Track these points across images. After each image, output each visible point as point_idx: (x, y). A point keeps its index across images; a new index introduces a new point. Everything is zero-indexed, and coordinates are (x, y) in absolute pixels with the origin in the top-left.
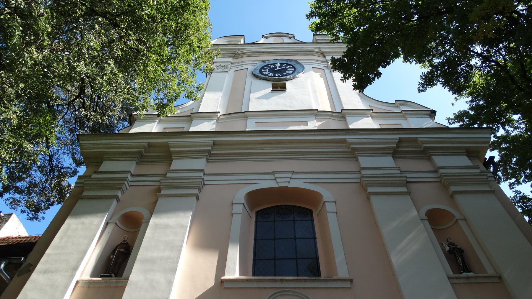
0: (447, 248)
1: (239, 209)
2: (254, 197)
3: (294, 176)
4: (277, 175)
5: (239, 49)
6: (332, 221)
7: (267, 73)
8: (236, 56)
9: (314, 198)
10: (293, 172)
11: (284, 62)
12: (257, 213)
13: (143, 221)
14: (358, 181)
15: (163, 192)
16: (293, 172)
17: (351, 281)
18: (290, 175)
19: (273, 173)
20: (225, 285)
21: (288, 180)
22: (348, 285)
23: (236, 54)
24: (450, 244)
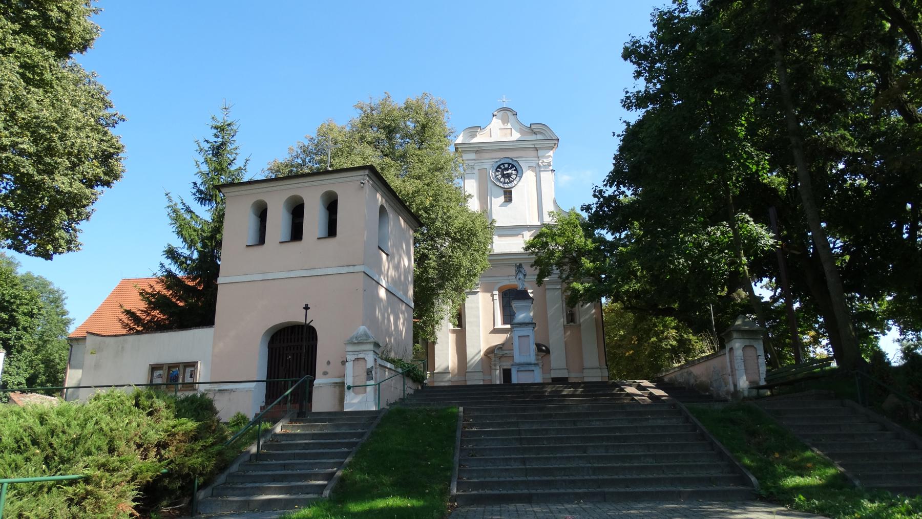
8: (477, 152)
11: (510, 162)
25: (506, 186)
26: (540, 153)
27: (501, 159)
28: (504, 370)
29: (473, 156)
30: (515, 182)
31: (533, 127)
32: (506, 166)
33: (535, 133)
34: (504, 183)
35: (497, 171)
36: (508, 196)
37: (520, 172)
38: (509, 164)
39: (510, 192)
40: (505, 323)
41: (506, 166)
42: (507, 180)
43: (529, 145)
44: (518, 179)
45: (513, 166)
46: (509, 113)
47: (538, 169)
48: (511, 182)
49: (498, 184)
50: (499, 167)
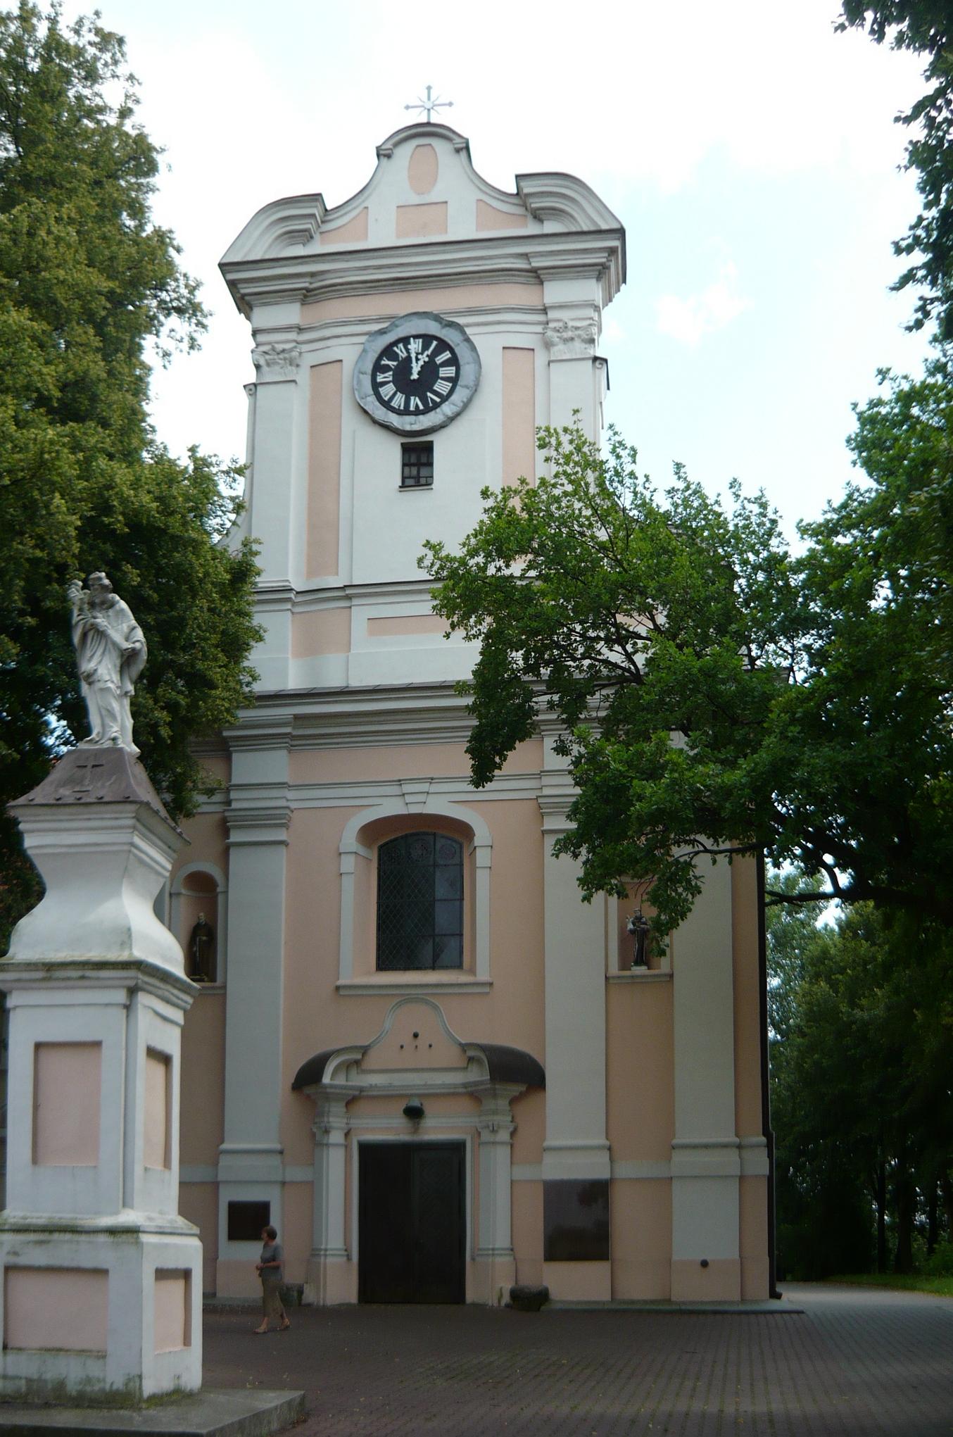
0: (630, 926)
1: (348, 864)
2: (370, 832)
3: (434, 788)
4: (407, 788)
5: (313, 275)
6: (482, 879)
7: (388, 391)
8: (307, 296)
9: (463, 831)
10: (431, 780)
11: (433, 328)
12: (381, 848)
13: (219, 889)
14: (533, 795)
15: (235, 837)
16: (431, 780)
17: (491, 984)
18: (425, 787)
19: (400, 782)
20: (342, 992)
21: (421, 798)
22: (487, 990)
25: (408, 423)
26: (555, 292)
27: (394, 320)
28: (367, 1151)
29: (290, 314)
30: (447, 409)
32: (415, 346)
34: (406, 412)
35: (378, 368)
36: (417, 461)
37: (467, 370)
38: (427, 339)
39: (428, 448)
40: (384, 963)
42: (415, 401)
44: (459, 396)
45: (443, 346)
46: (438, 144)
47: (541, 358)
48: (427, 410)
49: (380, 413)
50: (388, 352)
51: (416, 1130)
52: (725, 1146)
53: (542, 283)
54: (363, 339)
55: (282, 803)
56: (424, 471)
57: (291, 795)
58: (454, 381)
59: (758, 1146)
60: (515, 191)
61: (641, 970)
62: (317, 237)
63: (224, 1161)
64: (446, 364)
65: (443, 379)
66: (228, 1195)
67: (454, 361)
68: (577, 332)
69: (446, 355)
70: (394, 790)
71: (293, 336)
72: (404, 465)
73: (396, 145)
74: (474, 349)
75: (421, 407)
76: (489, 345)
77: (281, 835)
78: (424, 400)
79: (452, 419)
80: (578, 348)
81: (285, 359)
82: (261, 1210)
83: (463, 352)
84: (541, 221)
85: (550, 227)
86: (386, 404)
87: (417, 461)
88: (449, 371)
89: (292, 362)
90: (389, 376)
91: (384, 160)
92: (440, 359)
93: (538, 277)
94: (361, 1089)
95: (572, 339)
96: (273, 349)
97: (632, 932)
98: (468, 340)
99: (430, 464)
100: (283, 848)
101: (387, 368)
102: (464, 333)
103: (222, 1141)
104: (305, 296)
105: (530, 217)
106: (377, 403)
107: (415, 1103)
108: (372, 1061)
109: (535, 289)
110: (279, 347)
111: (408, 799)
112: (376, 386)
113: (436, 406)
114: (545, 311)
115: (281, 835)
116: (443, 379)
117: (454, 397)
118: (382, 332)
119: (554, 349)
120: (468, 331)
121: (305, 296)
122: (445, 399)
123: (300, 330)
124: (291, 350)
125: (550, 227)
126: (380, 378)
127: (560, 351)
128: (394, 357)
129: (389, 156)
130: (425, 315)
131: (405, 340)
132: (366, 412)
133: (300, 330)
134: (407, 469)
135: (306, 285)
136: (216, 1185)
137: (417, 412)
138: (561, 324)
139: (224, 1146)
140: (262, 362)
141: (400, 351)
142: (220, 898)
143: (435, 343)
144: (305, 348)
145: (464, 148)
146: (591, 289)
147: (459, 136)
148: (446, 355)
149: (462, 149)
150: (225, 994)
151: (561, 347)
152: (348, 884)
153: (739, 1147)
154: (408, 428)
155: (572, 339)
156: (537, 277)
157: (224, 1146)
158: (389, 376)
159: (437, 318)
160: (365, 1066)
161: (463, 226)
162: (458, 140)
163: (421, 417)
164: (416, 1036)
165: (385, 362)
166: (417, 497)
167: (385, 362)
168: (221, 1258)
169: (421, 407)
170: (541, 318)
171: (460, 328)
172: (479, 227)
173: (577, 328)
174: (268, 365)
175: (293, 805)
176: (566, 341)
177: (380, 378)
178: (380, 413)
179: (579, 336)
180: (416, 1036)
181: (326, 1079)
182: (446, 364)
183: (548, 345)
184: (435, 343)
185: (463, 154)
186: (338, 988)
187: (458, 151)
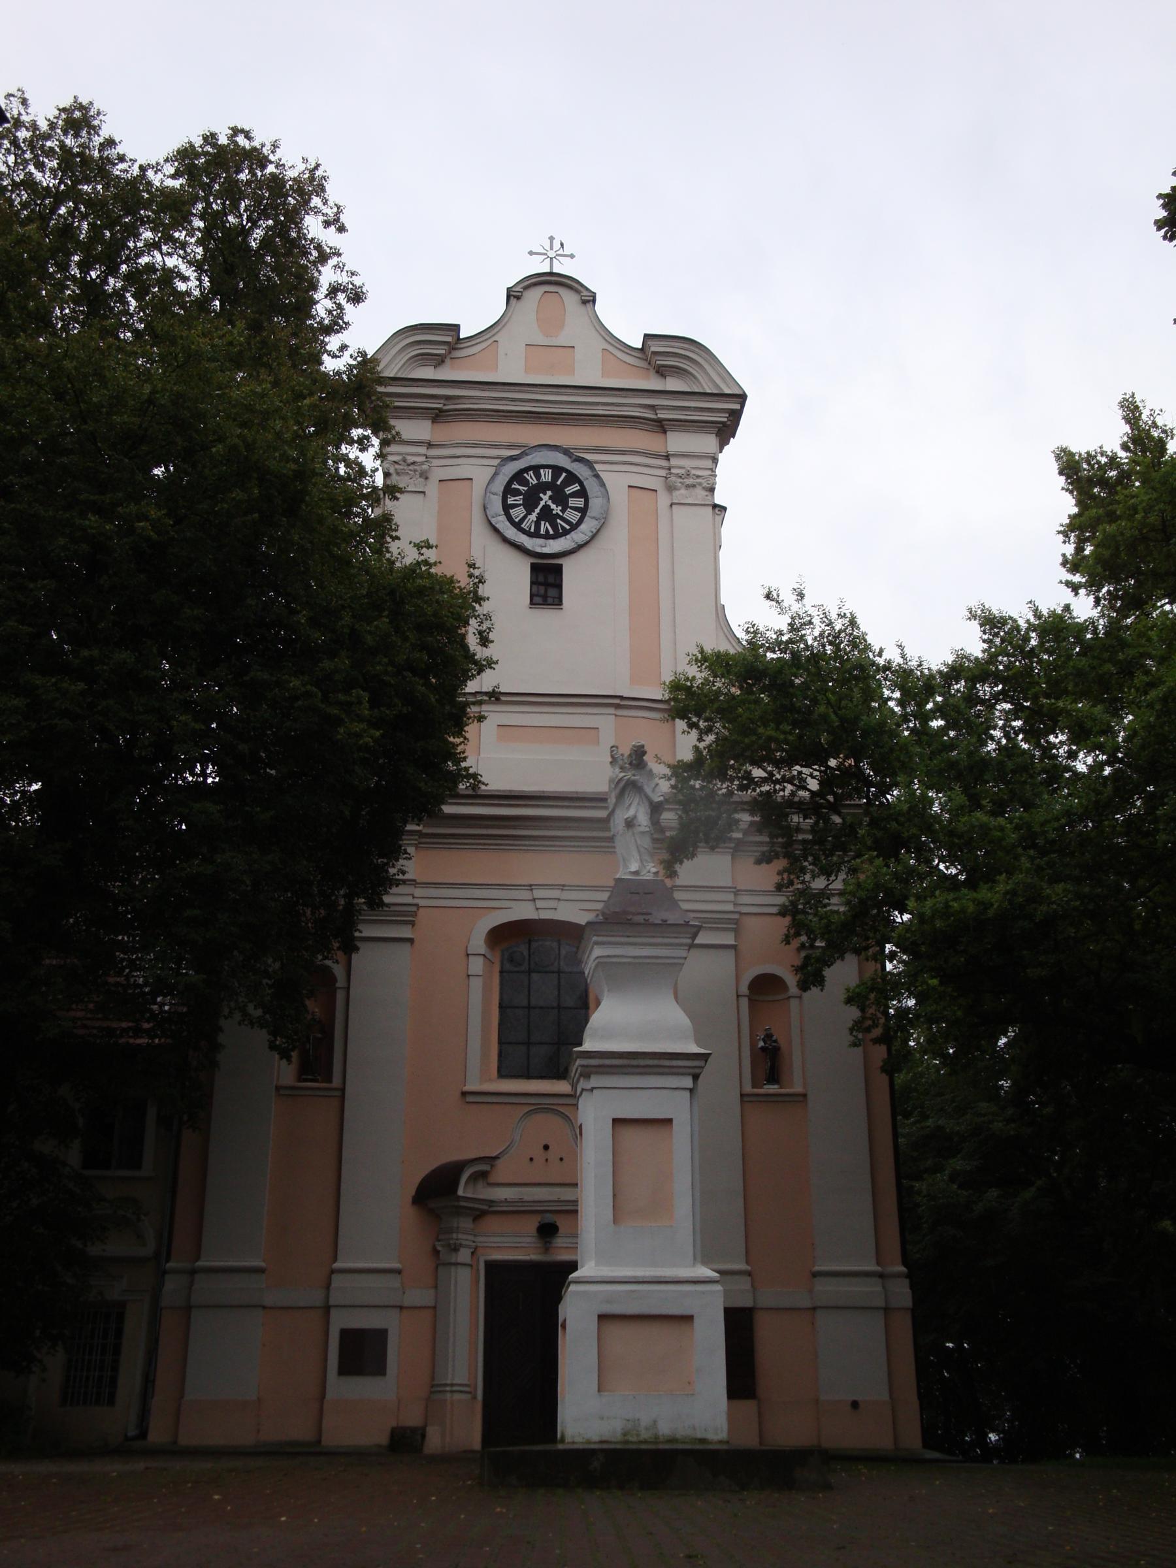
0: (761, 1044)
1: (477, 965)
2: (501, 935)
4: (538, 893)
5: (448, 398)
7: (518, 513)
8: (437, 417)
10: (562, 887)
13: (338, 985)
16: (562, 887)
18: (556, 893)
19: (531, 887)
20: (470, 1099)
21: (552, 904)
23: (440, 410)
24: (768, 1037)
26: (677, 442)
27: (527, 450)
28: (493, 1268)
30: (578, 536)
31: (655, 347)
32: (546, 475)
33: (661, 372)
34: (536, 534)
35: (508, 491)
36: (547, 583)
37: (595, 504)
38: (557, 470)
41: (546, 475)
43: (631, 407)
44: (587, 527)
45: (572, 478)
47: (663, 499)
49: (511, 533)
50: (518, 477)
51: (547, 1249)
52: (867, 1274)
53: (665, 432)
54: (496, 462)
55: (409, 900)
56: (552, 592)
57: (418, 892)
58: (583, 511)
59: (898, 1275)
60: (640, 346)
61: (773, 1089)
62: (448, 361)
63: (337, 1280)
64: (575, 495)
65: (572, 508)
66: (341, 1321)
67: (583, 493)
68: (699, 480)
69: (576, 487)
70: (525, 894)
71: (422, 450)
72: (532, 583)
73: (526, 288)
74: (603, 485)
75: (551, 532)
76: (617, 481)
77: (405, 932)
78: (554, 526)
79: (580, 547)
80: (700, 494)
81: (415, 471)
82: (381, 1336)
83: (591, 485)
84: (663, 376)
85: (673, 384)
86: (517, 525)
87: (547, 583)
88: (580, 503)
89: (425, 476)
90: (519, 499)
91: (513, 301)
92: (569, 490)
93: (662, 426)
94: (491, 1203)
95: (694, 486)
96: (405, 461)
97: (762, 1048)
98: (597, 476)
99: (559, 586)
100: (408, 944)
101: (516, 493)
102: (592, 469)
103: (335, 1260)
104: (437, 416)
105: (652, 372)
106: (508, 523)
107: (549, 1218)
108: (501, 1173)
109: (660, 437)
110: (410, 459)
111: (539, 904)
112: (507, 508)
113: (566, 533)
114: (667, 457)
115: (405, 932)
116: (572, 508)
117: (583, 527)
118: (513, 458)
119: (676, 493)
120: (597, 467)
121: (437, 416)
122: (574, 527)
123: (430, 445)
124: (422, 463)
125: (673, 384)
126: (510, 501)
127: (681, 495)
128: (525, 482)
129: (518, 298)
130: (555, 448)
131: (536, 469)
132: (496, 530)
133: (430, 445)
134: (535, 587)
135: (440, 406)
136: (327, 1309)
137: (547, 536)
138: (682, 471)
139: (336, 1265)
140: (392, 471)
141: (531, 478)
142: (340, 996)
143: (564, 475)
144: (436, 462)
145: (589, 299)
146: (708, 442)
147: (587, 289)
148: (576, 487)
149: (588, 301)
150: (343, 1097)
151: (683, 491)
152: (476, 985)
153: (881, 1276)
154: (539, 550)
155: (694, 486)
156: (661, 427)
157: (336, 1265)
158: (519, 499)
159: (566, 452)
160: (492, 1179)
161: (588, 371)
162: (585, 293)
163: (551, 541)
164: (546, 1147)
165: (515, 486)
166: (546, 616)
167: (515, 486)
168: (330, 1395)
169: (551, 532)
170: (664, 463)
171: (589, 464)
172: (604, 374)
173: (698, 477)
174: (398, 474)
175: (422, 902)
176: (688, 486)
177: (510, 501)
178: (511, 533)
179: (700, 484)
180: (546, 1147)
181: (460, 1192)
182: (575, 495)
183: (670, 489)
184: (564, 475)
185: (590, 305)
186: (464, 1094)
187: (584, 302)
